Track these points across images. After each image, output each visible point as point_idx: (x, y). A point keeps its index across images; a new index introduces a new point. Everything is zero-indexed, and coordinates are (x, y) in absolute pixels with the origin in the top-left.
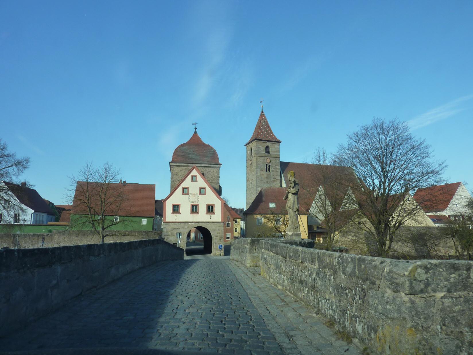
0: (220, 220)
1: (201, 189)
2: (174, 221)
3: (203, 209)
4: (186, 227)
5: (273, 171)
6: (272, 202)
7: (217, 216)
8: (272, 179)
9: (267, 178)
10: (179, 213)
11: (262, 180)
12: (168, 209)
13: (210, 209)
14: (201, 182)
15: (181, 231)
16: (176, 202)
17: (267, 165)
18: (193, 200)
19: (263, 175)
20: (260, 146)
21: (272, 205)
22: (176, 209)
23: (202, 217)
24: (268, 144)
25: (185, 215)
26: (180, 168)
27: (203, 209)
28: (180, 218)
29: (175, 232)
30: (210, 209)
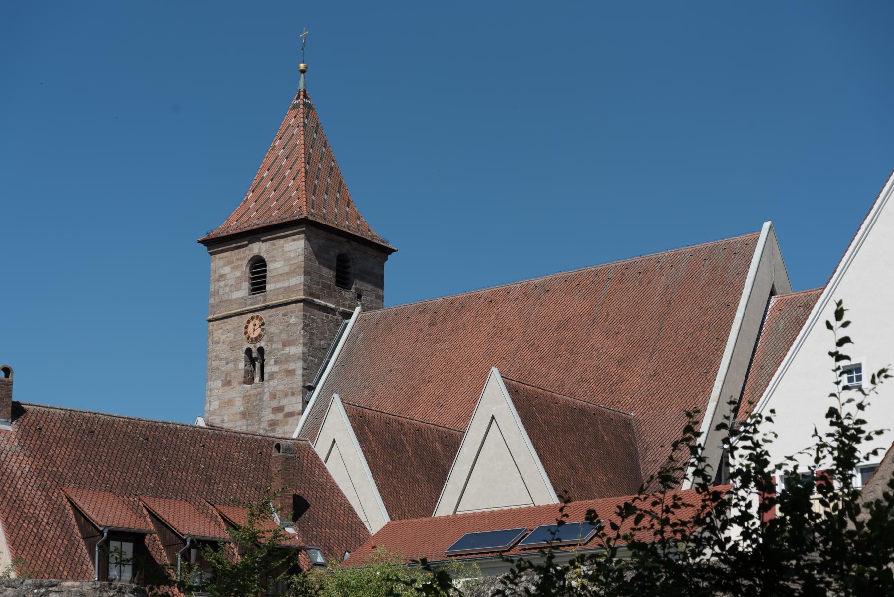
5: (272, 376)
17: (249, 351)
19: (230, 402)
20: (227, 270)
24: (257, 248)
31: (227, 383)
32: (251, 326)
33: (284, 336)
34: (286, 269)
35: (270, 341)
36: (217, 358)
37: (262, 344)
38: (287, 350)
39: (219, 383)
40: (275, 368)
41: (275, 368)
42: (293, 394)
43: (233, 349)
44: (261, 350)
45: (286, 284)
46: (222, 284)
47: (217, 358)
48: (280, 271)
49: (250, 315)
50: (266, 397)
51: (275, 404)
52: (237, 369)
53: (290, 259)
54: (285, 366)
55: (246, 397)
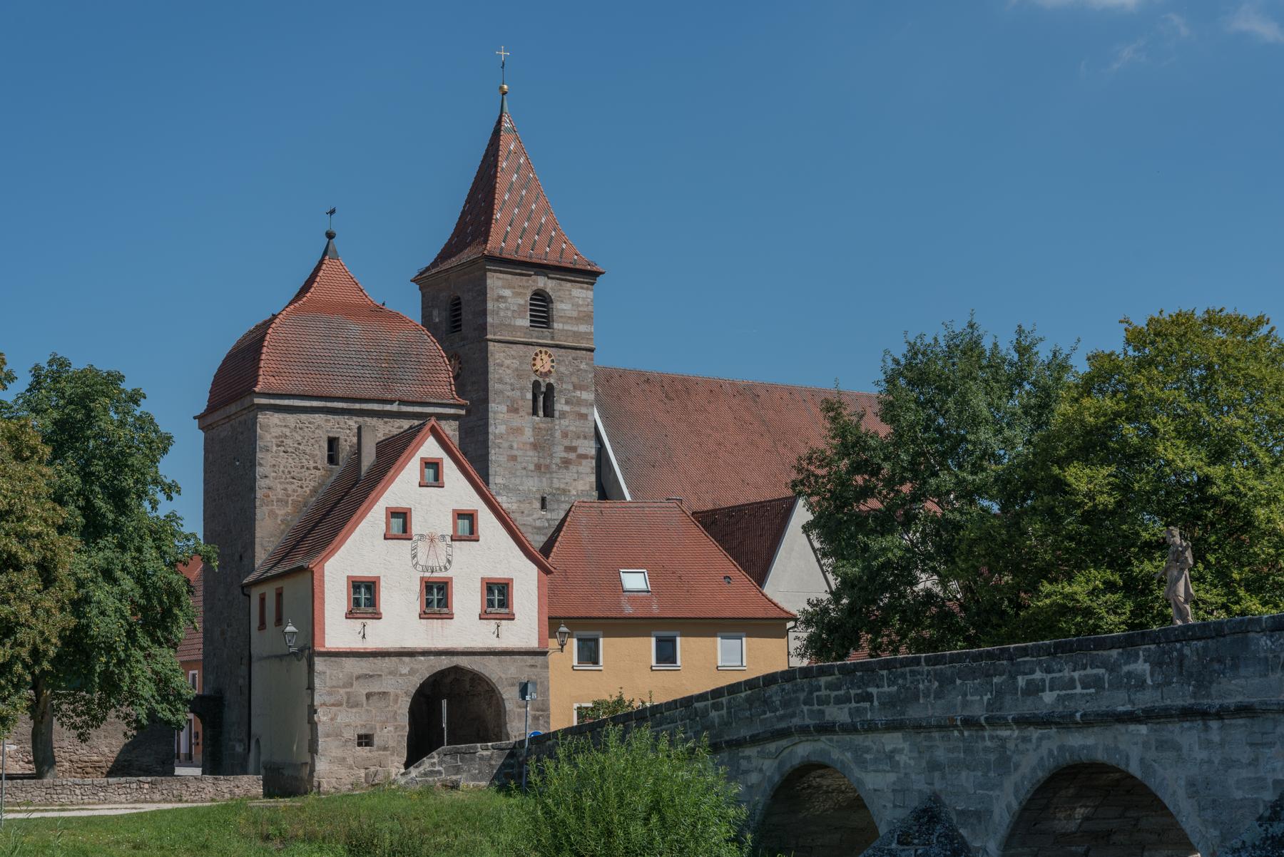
0: (533, 644)
1: (460, 515)
2: (358, 645)
3: (467, 599)
4: (405, 670)
5: (563, 415)
6: (633, 565)
7: (524, 628)
8: (560, 453)
9: (535, 446)
10: (377, 616)
11: (514, 458)
12: (335, 598)
13: (497, 596)
14: (458, 490)
15: (388, 684)
16: (363, 571)
17: (536, 385)
18: (433, 559)
19: (518, 431)
20: (507, 293)
21: (634, 581)
22: (365, 596)
23: (466, 629)
25: (400, 624)
26: (291, 419)
27: (467, 599)
28: (380, 635)
29: (361, 689)
30: (497, 596)
31: (514, 410)
32: (538, 362)
33: (574, 379)
34: (575, 314)
35: (560, 379)
36: (500, 381)
37: (552, 381)
38: (578, 393)
39: (505, 409)
40: (567, 408)
41: (567, 408)
42: (585, 438)
43: (519, 377)
44: (550, 387)
45: (575, 329)
46: (502, 305)
47: (500, 381)
48: (568, 314)
49: (538, 349)
50: (558, 434)
51: (567, 443)
52: (523, 398)
53: (578, 306)
54: (577, 409)
55: (536, 429)
